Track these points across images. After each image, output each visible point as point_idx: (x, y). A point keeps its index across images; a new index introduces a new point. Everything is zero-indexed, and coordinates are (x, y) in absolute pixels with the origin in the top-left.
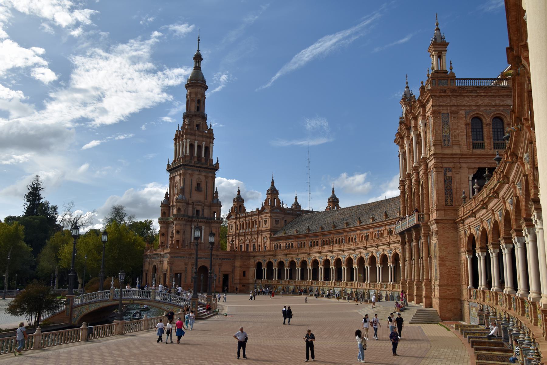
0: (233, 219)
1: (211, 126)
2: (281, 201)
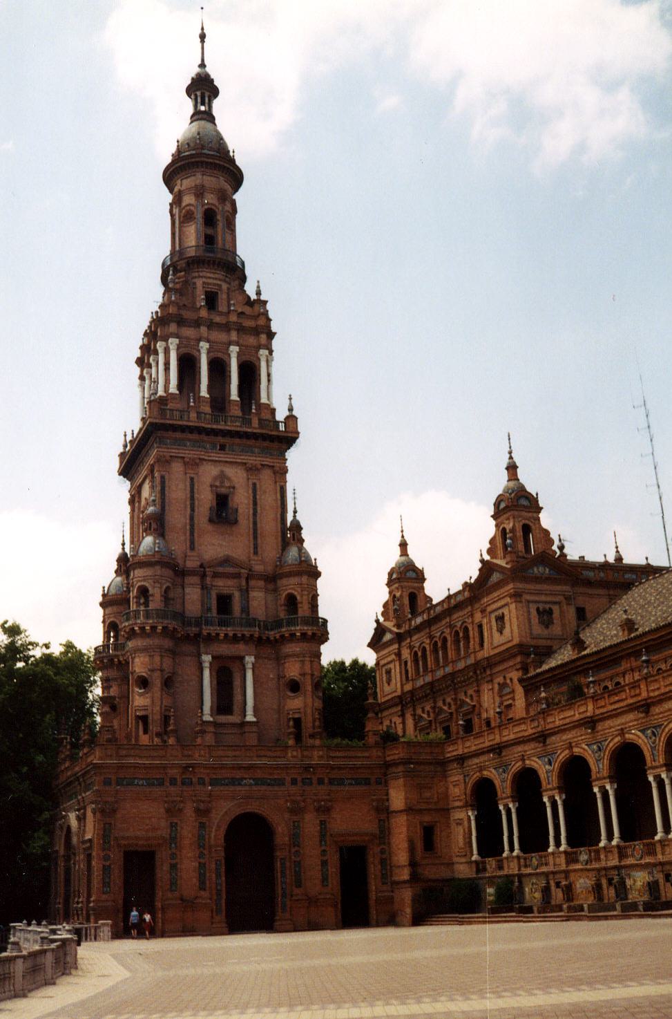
0: (390, 643)
1: (258, 293)
2: (554, 536)
